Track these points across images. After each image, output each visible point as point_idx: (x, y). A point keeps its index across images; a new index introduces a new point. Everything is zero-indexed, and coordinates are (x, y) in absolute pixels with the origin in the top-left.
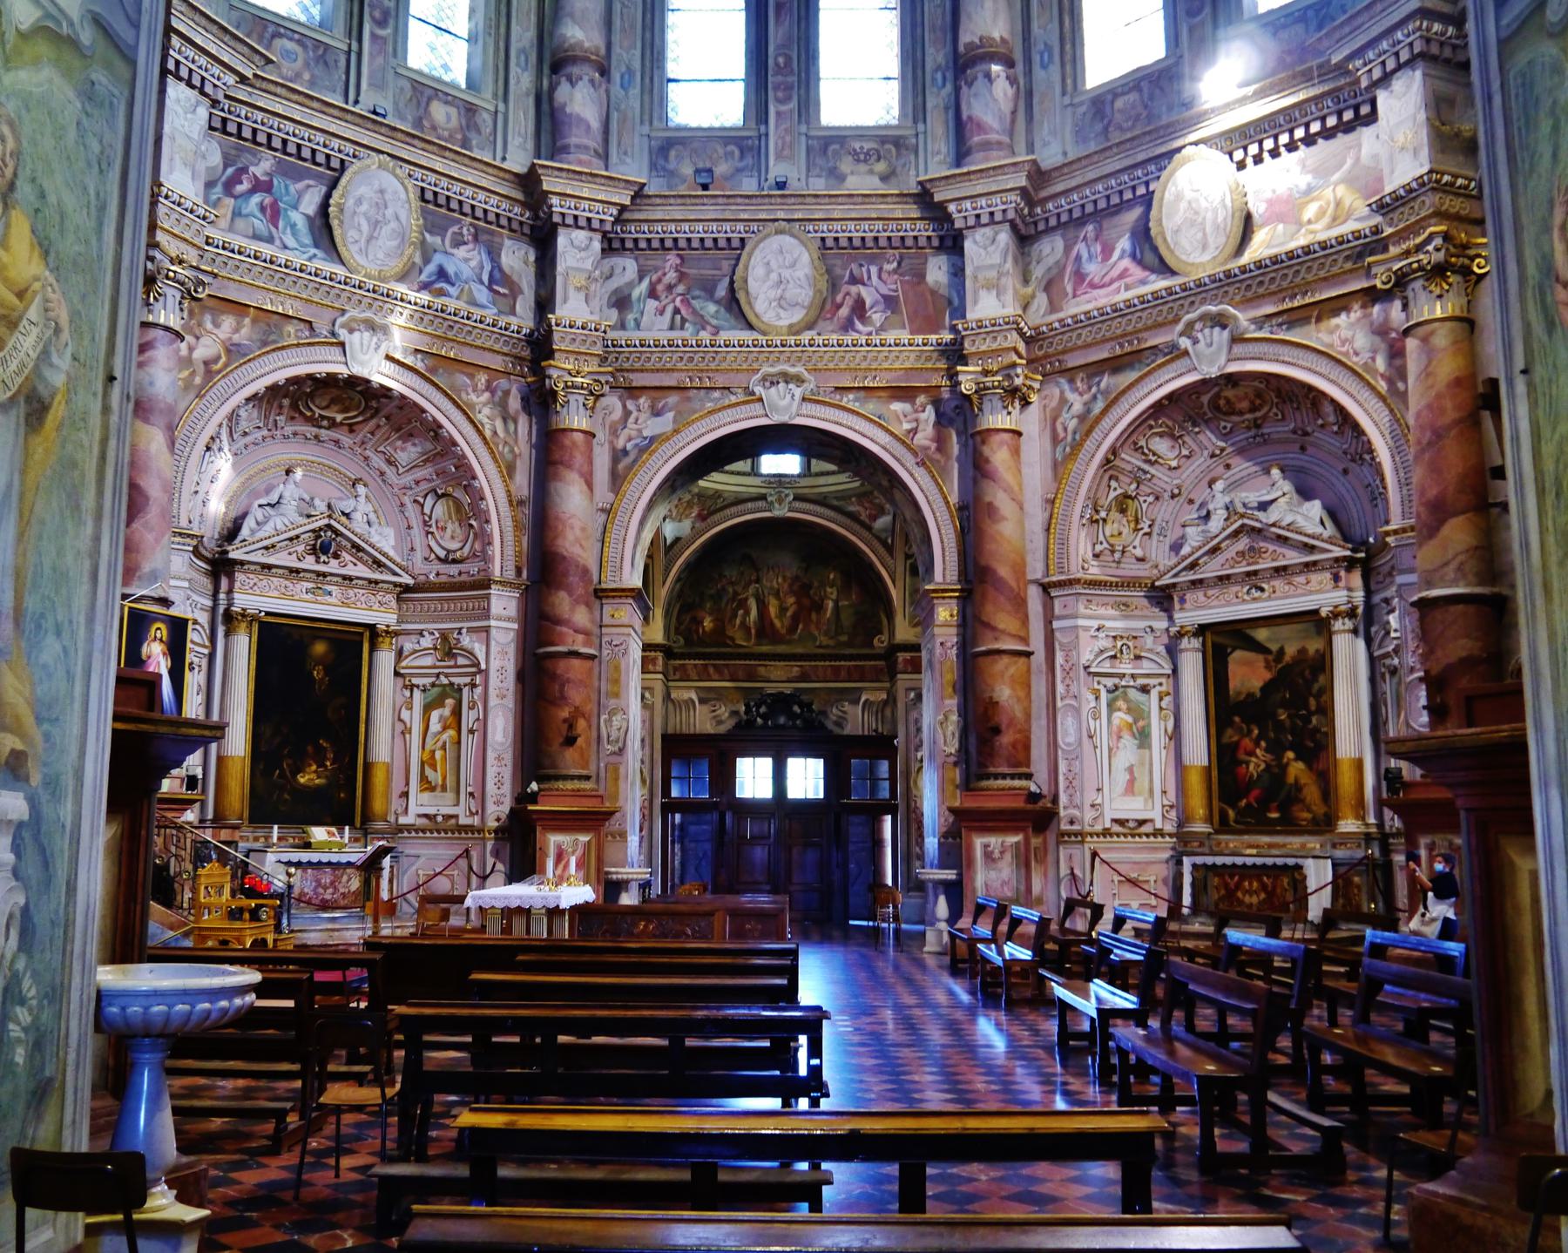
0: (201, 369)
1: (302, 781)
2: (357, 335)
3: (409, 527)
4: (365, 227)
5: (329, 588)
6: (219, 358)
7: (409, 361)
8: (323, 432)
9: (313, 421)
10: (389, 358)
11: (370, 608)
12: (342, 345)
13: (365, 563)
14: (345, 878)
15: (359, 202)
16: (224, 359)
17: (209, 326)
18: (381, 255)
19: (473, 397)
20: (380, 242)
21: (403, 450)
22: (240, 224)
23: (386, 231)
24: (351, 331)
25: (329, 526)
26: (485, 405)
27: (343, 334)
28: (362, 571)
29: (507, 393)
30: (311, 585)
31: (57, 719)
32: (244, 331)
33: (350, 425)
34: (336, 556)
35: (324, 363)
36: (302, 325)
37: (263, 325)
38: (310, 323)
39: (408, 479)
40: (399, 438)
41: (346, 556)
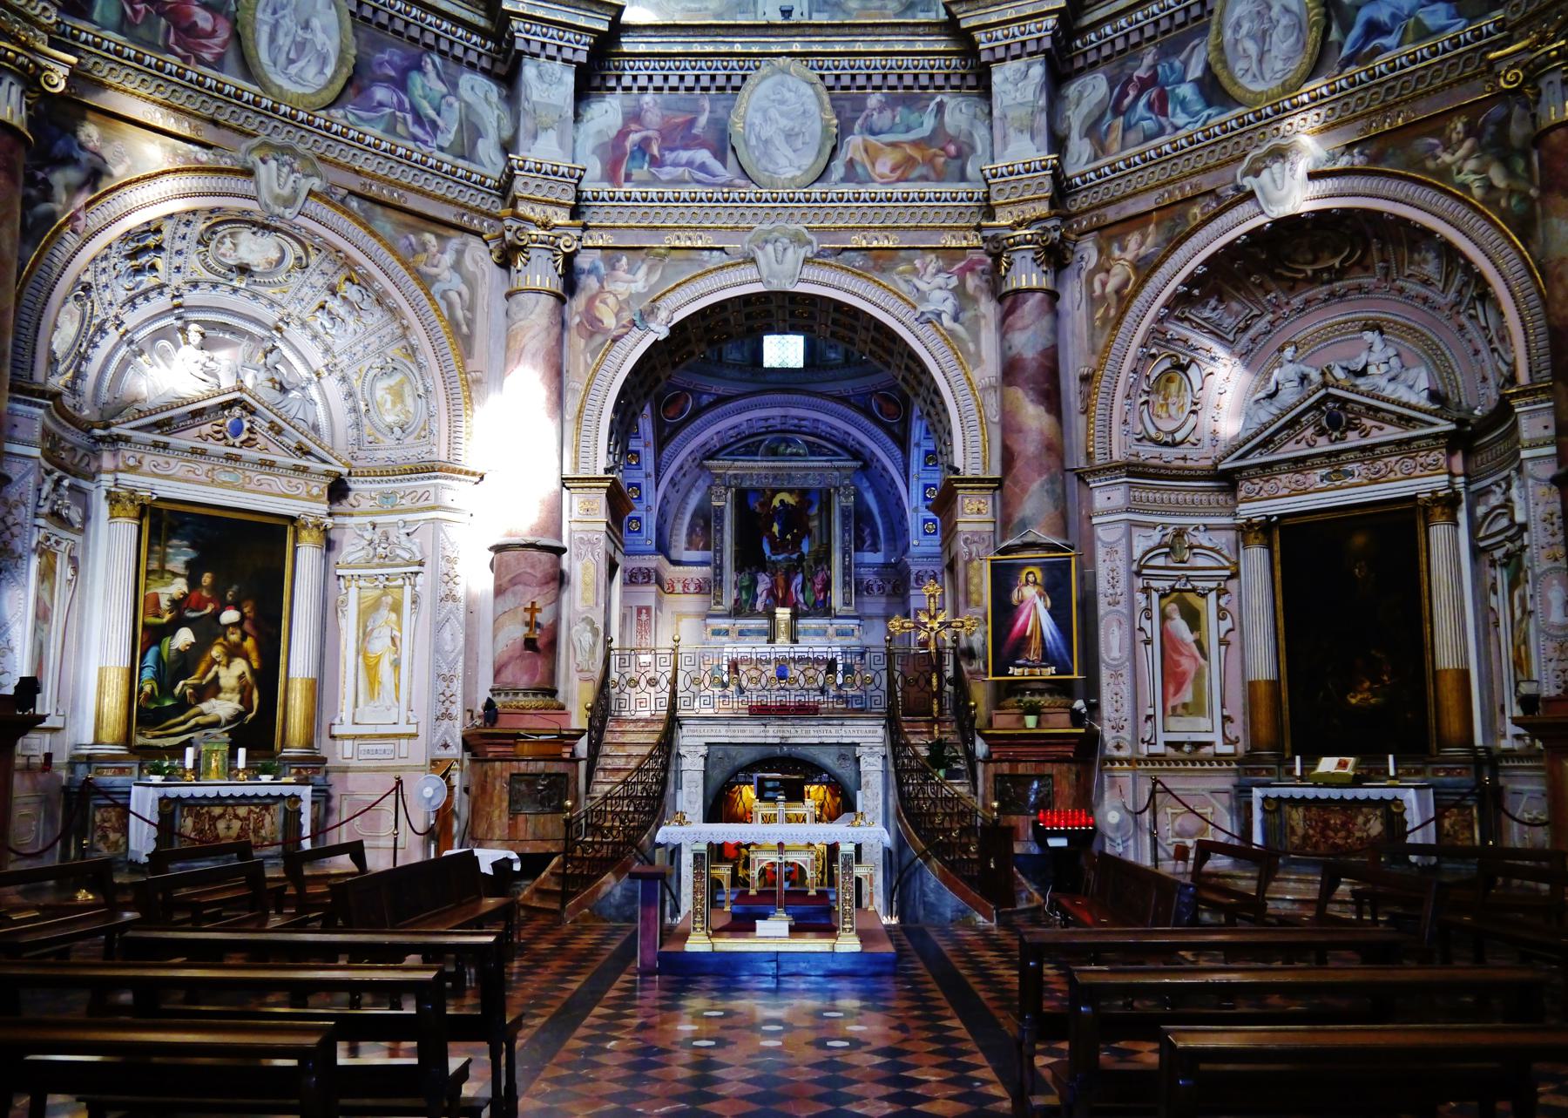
0: (1113, 300)
1: (1353, 701)
2: (1265, 174)
3: (1477, 352)
4: (1252, 47)
5: (1349, 467)
6: (1129, 279)
7: (1342, 163)
8: (1337, 285)
9: (1314, 280)
10: (1313, 176)
11: (1409, 477)
12: (1251, 195)
13: (1390, 423)
14: (1360, 820)
15: (1238, 26)
16: (1133, 278)
17: (1117, 253)
18: (1279, 65)
19: (1447, 158)
20: (1273, 53)
21: (1425, 261)
22: (1132, 136)
23: (1276, 36)
24: (1257, 174)
25: (1328, 396)
26: (1466, 158)
27: (1249, 183)
28: (1392, 433)
29: (1504, 123)
30: (1324, 471)
31: (563, 708)
32: (1150, 240)
33: (1359, 263)
34: (1351, 427)
35: (1239, 224)
36: (1208, 199)
37: (1168, 224)
38: (1212, 192)
39: (1452, 295)
40: (1411, 251)
41: (1368, 423)
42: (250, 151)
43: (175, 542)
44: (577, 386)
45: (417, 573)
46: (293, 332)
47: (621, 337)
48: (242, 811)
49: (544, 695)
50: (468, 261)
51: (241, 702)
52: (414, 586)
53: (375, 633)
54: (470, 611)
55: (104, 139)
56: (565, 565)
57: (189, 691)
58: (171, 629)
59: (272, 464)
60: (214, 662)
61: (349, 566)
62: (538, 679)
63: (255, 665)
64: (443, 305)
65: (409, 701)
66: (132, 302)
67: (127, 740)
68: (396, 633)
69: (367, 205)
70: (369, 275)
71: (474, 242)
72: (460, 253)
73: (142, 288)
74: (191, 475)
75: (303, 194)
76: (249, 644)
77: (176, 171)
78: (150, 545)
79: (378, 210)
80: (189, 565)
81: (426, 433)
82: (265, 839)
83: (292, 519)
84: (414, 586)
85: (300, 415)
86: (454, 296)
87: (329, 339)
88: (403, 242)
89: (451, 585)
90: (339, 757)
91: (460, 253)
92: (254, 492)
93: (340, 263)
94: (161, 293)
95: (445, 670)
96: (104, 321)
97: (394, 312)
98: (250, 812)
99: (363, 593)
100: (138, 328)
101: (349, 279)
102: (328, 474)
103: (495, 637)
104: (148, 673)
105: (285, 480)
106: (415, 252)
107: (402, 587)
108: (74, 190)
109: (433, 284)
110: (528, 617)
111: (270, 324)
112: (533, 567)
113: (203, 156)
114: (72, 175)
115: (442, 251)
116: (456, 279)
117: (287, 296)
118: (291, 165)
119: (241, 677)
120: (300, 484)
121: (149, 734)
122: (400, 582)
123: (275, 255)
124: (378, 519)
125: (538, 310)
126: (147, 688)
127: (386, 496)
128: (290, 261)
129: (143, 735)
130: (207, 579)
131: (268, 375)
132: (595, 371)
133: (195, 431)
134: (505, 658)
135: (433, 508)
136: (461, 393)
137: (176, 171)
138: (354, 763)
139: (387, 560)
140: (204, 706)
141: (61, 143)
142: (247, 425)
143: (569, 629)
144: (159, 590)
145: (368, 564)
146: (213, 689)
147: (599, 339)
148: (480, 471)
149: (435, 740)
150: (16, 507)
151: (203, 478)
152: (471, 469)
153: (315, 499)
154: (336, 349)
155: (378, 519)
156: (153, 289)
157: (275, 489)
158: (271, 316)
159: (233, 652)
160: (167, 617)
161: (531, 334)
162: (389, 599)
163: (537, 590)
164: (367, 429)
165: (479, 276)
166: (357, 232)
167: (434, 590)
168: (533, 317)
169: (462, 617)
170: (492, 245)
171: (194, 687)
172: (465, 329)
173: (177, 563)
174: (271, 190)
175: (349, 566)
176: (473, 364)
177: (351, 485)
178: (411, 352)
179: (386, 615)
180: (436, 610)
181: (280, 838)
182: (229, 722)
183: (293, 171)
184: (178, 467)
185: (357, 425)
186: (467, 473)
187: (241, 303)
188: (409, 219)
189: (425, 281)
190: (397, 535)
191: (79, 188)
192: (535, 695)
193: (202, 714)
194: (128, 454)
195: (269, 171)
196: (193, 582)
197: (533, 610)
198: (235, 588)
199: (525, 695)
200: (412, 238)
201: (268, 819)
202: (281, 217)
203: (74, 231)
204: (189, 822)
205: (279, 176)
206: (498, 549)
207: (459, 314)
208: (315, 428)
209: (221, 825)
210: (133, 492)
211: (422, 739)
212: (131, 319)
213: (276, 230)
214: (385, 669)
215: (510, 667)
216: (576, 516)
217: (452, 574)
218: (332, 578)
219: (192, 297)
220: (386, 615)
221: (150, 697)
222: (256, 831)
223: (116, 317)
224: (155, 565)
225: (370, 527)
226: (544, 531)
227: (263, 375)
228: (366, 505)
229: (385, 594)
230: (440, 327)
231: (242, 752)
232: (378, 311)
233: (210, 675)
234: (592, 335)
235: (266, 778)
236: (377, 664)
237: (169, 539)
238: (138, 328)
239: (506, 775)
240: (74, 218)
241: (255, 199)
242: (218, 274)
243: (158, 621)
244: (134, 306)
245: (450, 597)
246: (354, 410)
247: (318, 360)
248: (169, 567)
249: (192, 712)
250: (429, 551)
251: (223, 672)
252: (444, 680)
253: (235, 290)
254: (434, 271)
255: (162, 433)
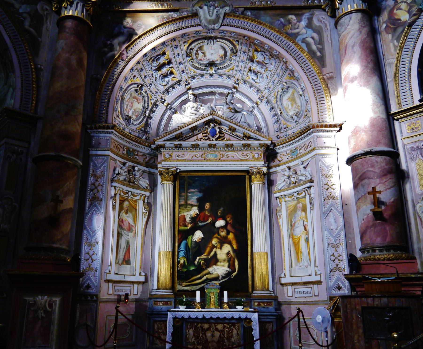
42: (194, 6)
43: (191, 190)
44: (392, 60)
45: (310, 187)
46: (242, 87)
47: (414, 21)
48: (220, 327)
49: (395, 250)
50: (315, 22)
51: (229, 267)
52: (310, 195)
53: (296, 225)
54: (344, 204)
55: (134, 22)
56: (404, 166)
57: (202, 262)
58: (192, 232)
59: (231, 146)
60: (214, 247)
61: (280, 190)
62: (388, 239)
63: (235, 247)
64: (304, 46)
65: (315, 261)
66: (167, 91)
67: (173, 288)
68: (305, 223)
69: (255, 12)
70: (262, 42)
71: (317, 12)
72: (310, 20)
73: (170, 84)
74: (194, 158)
75: (222, 17)
76: (231, 236)
77: (163, 24)
78: (180, 193)
79: (262, 12)
80: (198, 200)
81: (308, 113)
82: (234, 343)
83: (248, 172)
84: (310, 195)
85: (242, 120)
86: (310, 40)
87: (257, 85)
88: (277, 23)
89: (330, 190)
90: (286, 295)
91: (310, 20)
92: (224, 160)
93: (248, 44)
94: (180, 84)
95: (333, 241)
96: (156, 101)
97: (278, 57)
98: (224, 327)
99: (288, 205)
100: (173, 102)
101: (256, 50)
102: (261, 146)
103: (357, 215)
104: (182, 254)
105: (240, 153)
106: (284, 25)
107: (304, 197)
108: (121, 44)
109: (297, 37)
110: (372, 196)
111: (231, 87)
112: (373, 166)
113: (175, 15)
114: (121, 39)
115: (300, 21)
116: (310, 32)
117: (234, 71)
118: (214, 5)
119: (228, 254)
120: (249, 153)
121: (184, 284)
122: (304, 194)
123: (222, 52)
124: (291, 164)
125: (351, 22)
126: (182, 261)
127: (293, 151)
128: (229, 53)
129: (181, 285)
130: (207, 206)
131: (228, 106)
132: (401, 49)
133: (195, 138)
134: (364, 228)
135: (313, 150)
136: (322, 86)
137: (163, 24)
138: (293, 299)
139: (297, 183)
140: (210, 270)
141: (117, 29)
142: (218, 130)
143: (414, 206)
144: (185, 214)
145: (289, 188)
146: (214, 260)
147: (400, 30)
148: (338, 122)
149: (331, 284)
150: (100, 178)
151: (200, 158)
152: (332, 123)
153: (257, 160)
154: (262, 89)
155: (291, 164)
156: (176, 83)
157: (236, 158)
158: (230, 83)
159: (223, 241)
160: (190, 226)
161: (350, 36)
162: (300, 205)
163: (378, 181)
164: (283, 122)
165: (323, 26)
166: (252, 25)
167: (320, 194)
168: (349, 27)
169: (340, 208)
170: (327, 10)
171: (204, 260)
172: (318, 54)
173: (193, 200)
174: (206, 19)
175: (280, 190)
176: (325, 70)
177: (278, 151)
178: (292, 74)
179: (300, 214)
180: (322, 206)
181: (242, 343)
182: (223, 278)
183: (215, 7)
184: (188, 155)
185: (278, 122)
186: (331, 126)
187: (216, 80)
188: (278, 12)
189: (293, 37)
190: (300, 169)
191: (124, 43)
192: (388, 250)
193: (209, 273)
194: (165, 153)
195: (204, 11)
196: (201, 208)
197: (374, 192)
198: (222, 209)
199: (381, 251)
200: (282, 20)
201: (235, 331)
202: (213, 29)
203: (122, 60)
204: (191, 332)
205: (209, 12)
206: (350, 161)
207: (314, 47)
208: (259, 129)
209: (209, 334)
210: (168, 169)
211: (324, 285)
212: (169, 98)
213: (216, 38)
214: (303, 243)
215: (368, 233)
216: (405, 135)
217: (330, 184)
218: (273, 200)
219: (194, 83)
220: (300, 214)
221: (183, 266)
222: (229, 338)
223: (162, 98)
224: (182, 202)
225: (287, 169)
226: (378, 143)
227: (225, 107)
228: (285, 159)
229: (299, 203)
230: (305, 56)
231: (225, 293)
232: (273, 61)
233: (212, 254)
234: (395, 30)
235: (240, 308)
236: (299, 242)
237: (189, 189)
238: (173, 102)
239: (359, 307)
240: (122, 54)
241: (200, 25)
242: (201, 69)
243: (185, 228)
244: (168, 92)
245: (331, 197)
246: (275, 115)
247: (255, 97)
248: (189, 202)
249: (204, 272)
250: (315, 174)
251: (218, 251)
252: (333, 246)
253: (211, 75)
254: (296, 31)
255: (179, 141)
